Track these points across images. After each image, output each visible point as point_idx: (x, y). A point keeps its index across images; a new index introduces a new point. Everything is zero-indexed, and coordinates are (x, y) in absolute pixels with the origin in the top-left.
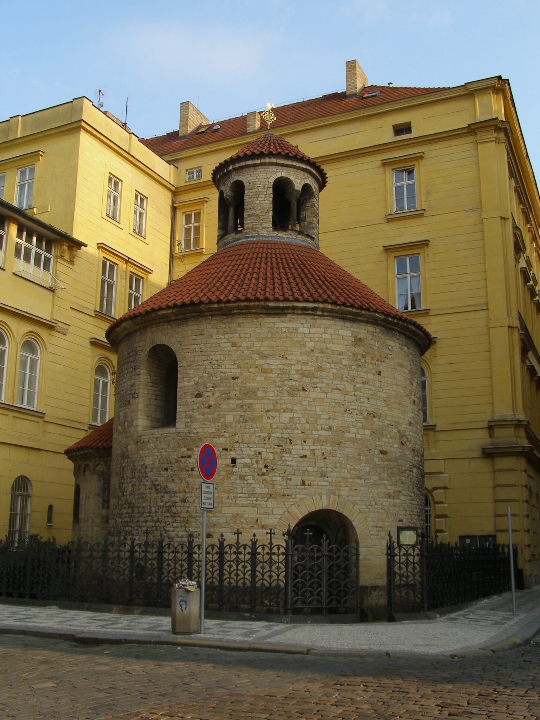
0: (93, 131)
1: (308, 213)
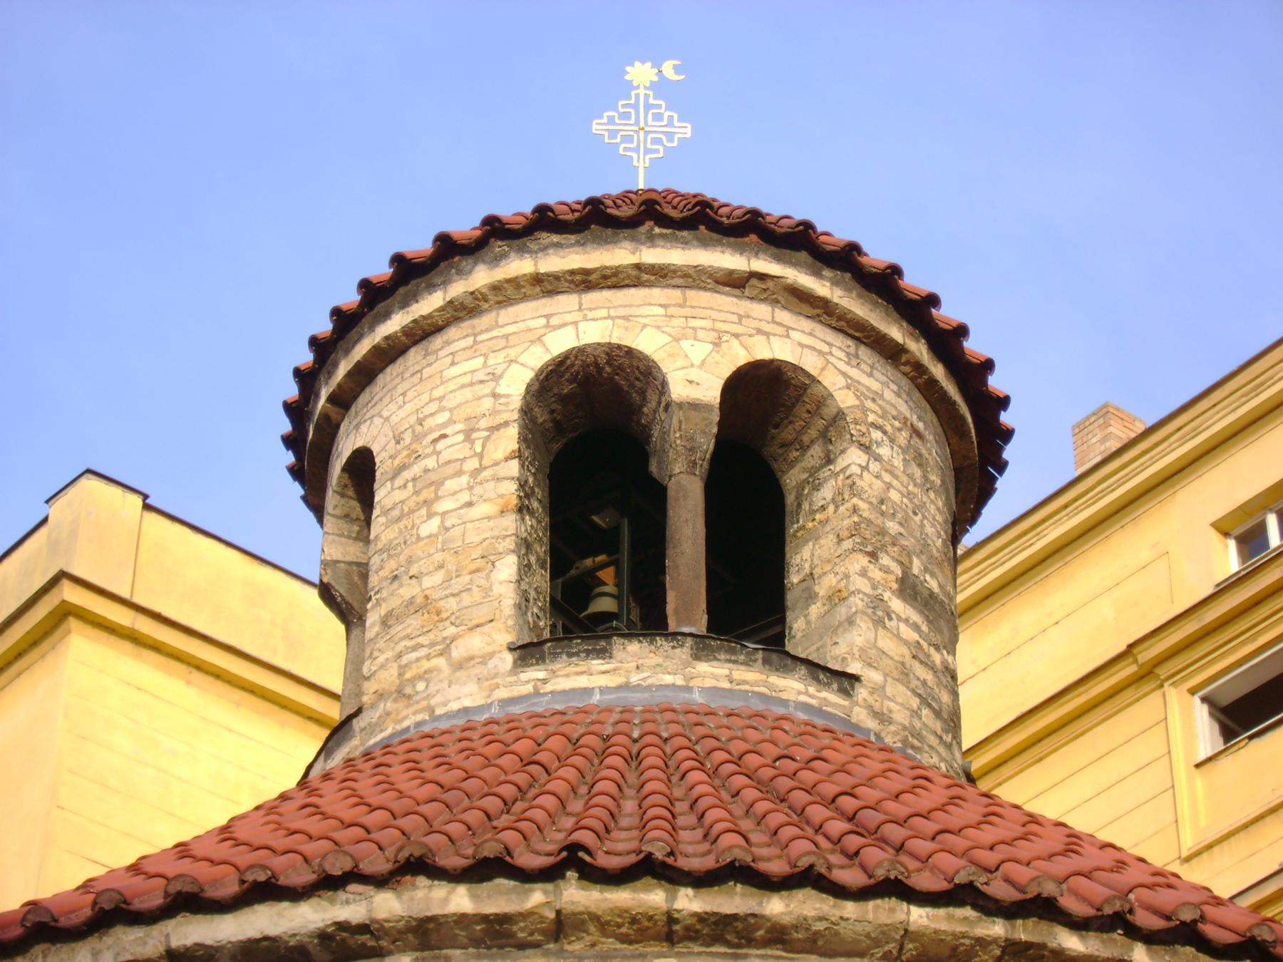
0: (146, 627)
1: (828, 541)
